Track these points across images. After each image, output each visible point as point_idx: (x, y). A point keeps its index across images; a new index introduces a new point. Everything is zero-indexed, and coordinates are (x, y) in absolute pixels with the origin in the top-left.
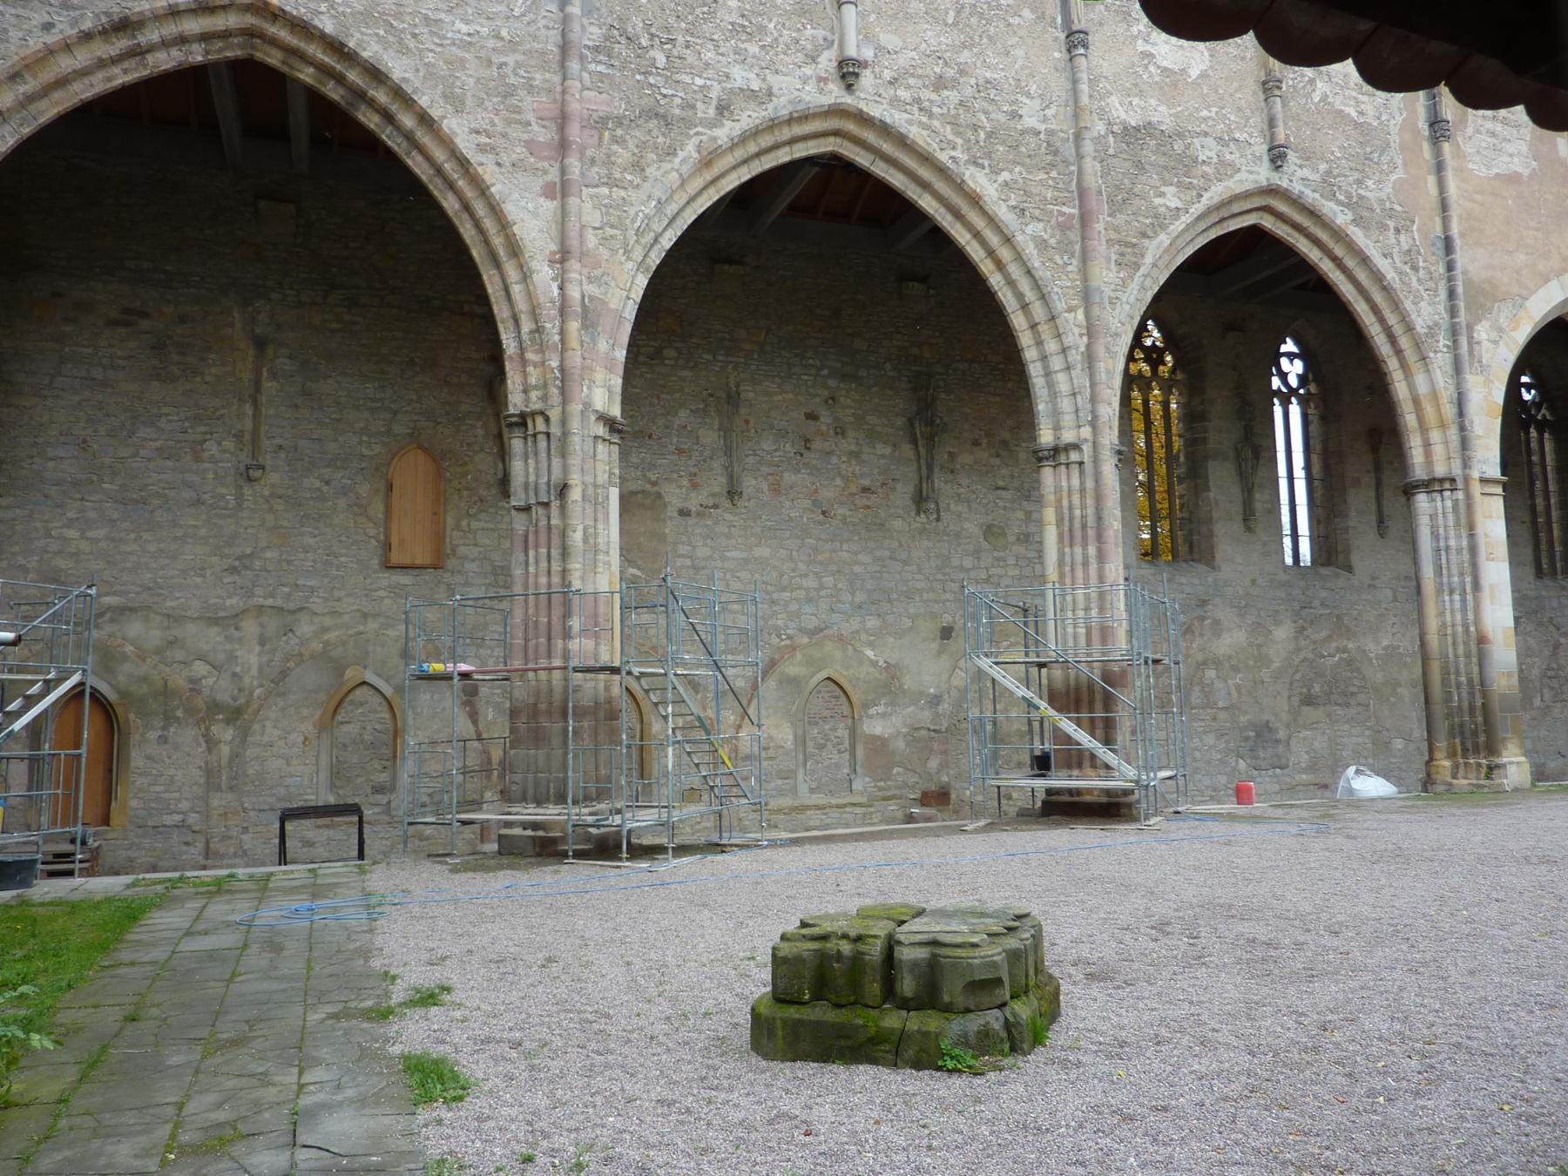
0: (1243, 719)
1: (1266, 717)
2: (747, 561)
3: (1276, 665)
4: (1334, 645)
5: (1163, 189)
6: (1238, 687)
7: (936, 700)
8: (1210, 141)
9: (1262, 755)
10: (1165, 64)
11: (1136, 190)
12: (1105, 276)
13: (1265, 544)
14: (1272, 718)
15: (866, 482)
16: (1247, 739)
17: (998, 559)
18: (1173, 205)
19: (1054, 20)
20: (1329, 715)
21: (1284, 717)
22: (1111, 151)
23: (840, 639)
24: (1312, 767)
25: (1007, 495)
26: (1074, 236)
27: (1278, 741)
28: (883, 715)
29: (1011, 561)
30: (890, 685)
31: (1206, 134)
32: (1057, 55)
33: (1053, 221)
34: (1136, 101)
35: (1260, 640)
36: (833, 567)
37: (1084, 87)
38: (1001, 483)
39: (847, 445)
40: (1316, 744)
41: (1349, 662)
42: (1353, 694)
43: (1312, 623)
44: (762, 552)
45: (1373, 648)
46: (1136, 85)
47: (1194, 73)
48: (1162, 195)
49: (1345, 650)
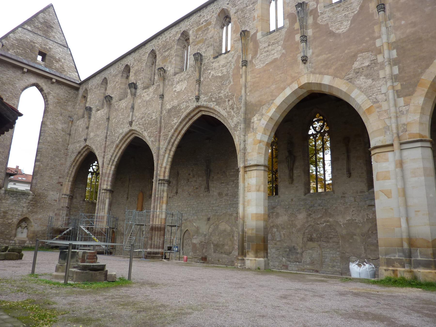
0: (285, 245)
1: (293, 245)
2: (177, 206)
3: (299, 226)
4: (323, 220)
6: (284, 234)
7: (205, 235)
9: (291, 257)
13: (297, 187)
14: (296, 245)
15: (197, 187)
16: (286, 251)
17: (221, 201)
20: (320, 245)
21: (301, 245)
23: (190, 221)
24: (312, 263)
25: (224, 184)
27: (297, 253)
28: (196, 238)
29: (223, 201)
30: (197, 231)
35: (293, 219)
36: (190, 206)
38: (223, 182)
39: (195, 179)
40: (314, 256)
41: (330, 226)
42: (331, 238)
43: (314, 212)
44: (180, 204)
45: (342, 220)
47: (183, 89)
49: (328, 221)
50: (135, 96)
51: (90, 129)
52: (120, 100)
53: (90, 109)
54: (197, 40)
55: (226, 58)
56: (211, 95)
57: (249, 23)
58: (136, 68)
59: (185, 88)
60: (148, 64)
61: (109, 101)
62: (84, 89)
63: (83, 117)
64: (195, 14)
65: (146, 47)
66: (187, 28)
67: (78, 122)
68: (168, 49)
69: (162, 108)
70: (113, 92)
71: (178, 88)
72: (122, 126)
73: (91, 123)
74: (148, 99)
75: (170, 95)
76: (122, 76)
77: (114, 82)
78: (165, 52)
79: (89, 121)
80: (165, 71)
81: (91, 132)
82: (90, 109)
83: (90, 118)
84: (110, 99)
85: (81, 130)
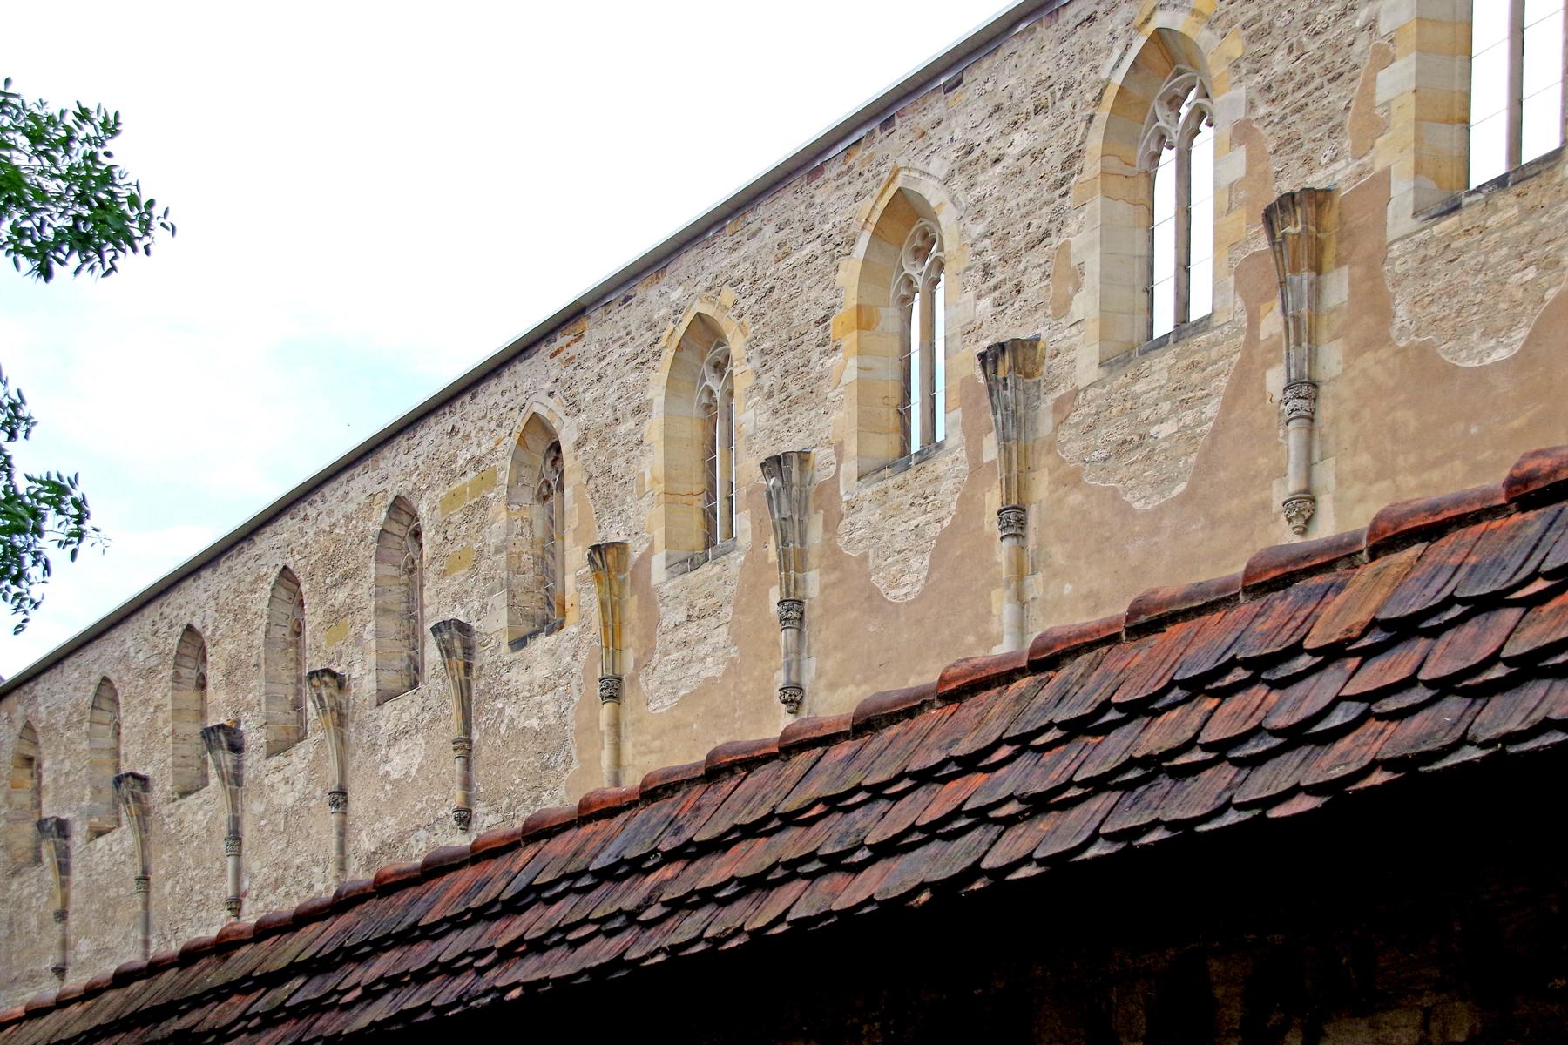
47: (413, 771)
50: (239, 785)
51: (73, 920)
52: (185, 794)
53: (62, 828)
54: (450, 550)
55: (552, 652)
56: (509, 808)
57: (623, 502)
58: (228, 647)
59: (421, 767)
60: (278, 633)
61: (137, 798)
62: (19, 725)
63: (38, 860)
65: (256, 551)
67: (14, 886)
68: (346, 576)
69: (342, 848)
70: (148, 753)
72: (204, 914)
73: (76, 896)
74: (290, 800)
75: (370, 793)
76: (177, 677)
77: (145, 702)
78: (335, 586)
79: (64, 884)
80: (340, 682)
81: (78, 935)
82: (62, 828)
83: (64, 868)
84: (138, 790)
85: (34, 922)
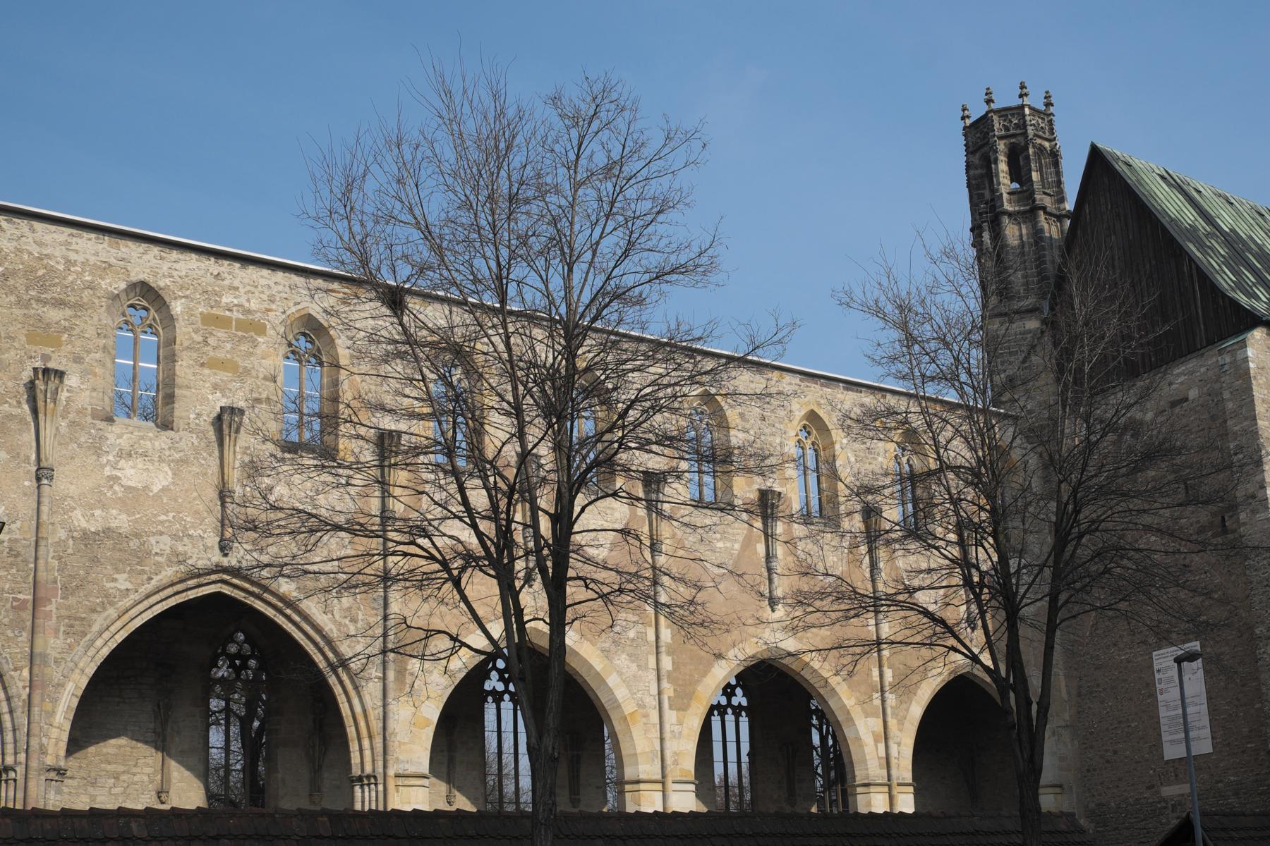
5: (116, 576)
8: (166, 539)
10: (130, 483)
11: (90, 579)
12: (52, 644)
18: (123, 587)
19: (28, 458)
22: (70, 551)
26: (27, 615)
31: (161, 533)
32: (26, 483)
33: (8, 606)
34: (98, 512)
37: (45, 509)
46: (99, 501)
47: (156, 489)
48: (115, 580)
64: (193, 256)
66: (162, 284)
71: (131, 474)
